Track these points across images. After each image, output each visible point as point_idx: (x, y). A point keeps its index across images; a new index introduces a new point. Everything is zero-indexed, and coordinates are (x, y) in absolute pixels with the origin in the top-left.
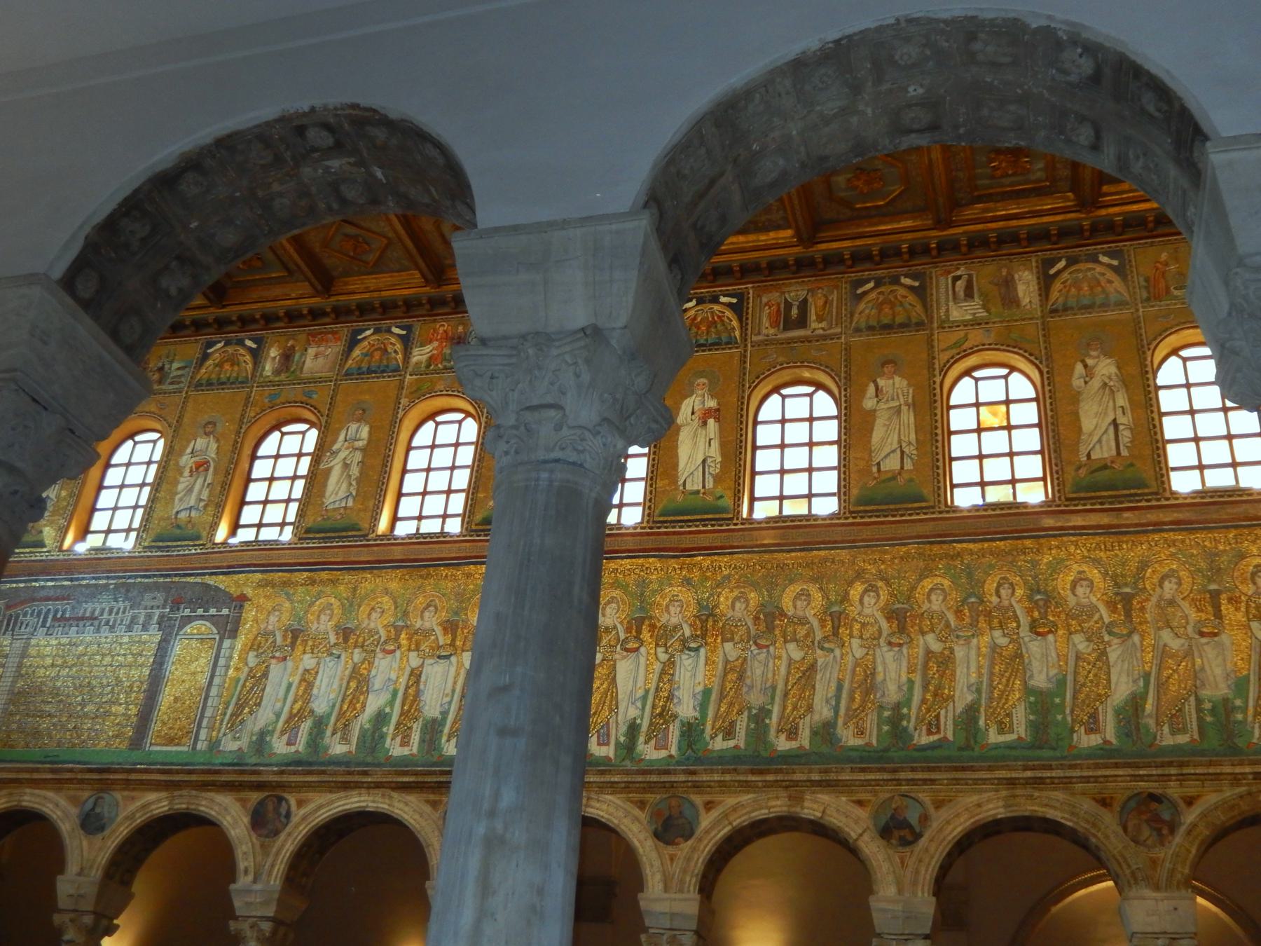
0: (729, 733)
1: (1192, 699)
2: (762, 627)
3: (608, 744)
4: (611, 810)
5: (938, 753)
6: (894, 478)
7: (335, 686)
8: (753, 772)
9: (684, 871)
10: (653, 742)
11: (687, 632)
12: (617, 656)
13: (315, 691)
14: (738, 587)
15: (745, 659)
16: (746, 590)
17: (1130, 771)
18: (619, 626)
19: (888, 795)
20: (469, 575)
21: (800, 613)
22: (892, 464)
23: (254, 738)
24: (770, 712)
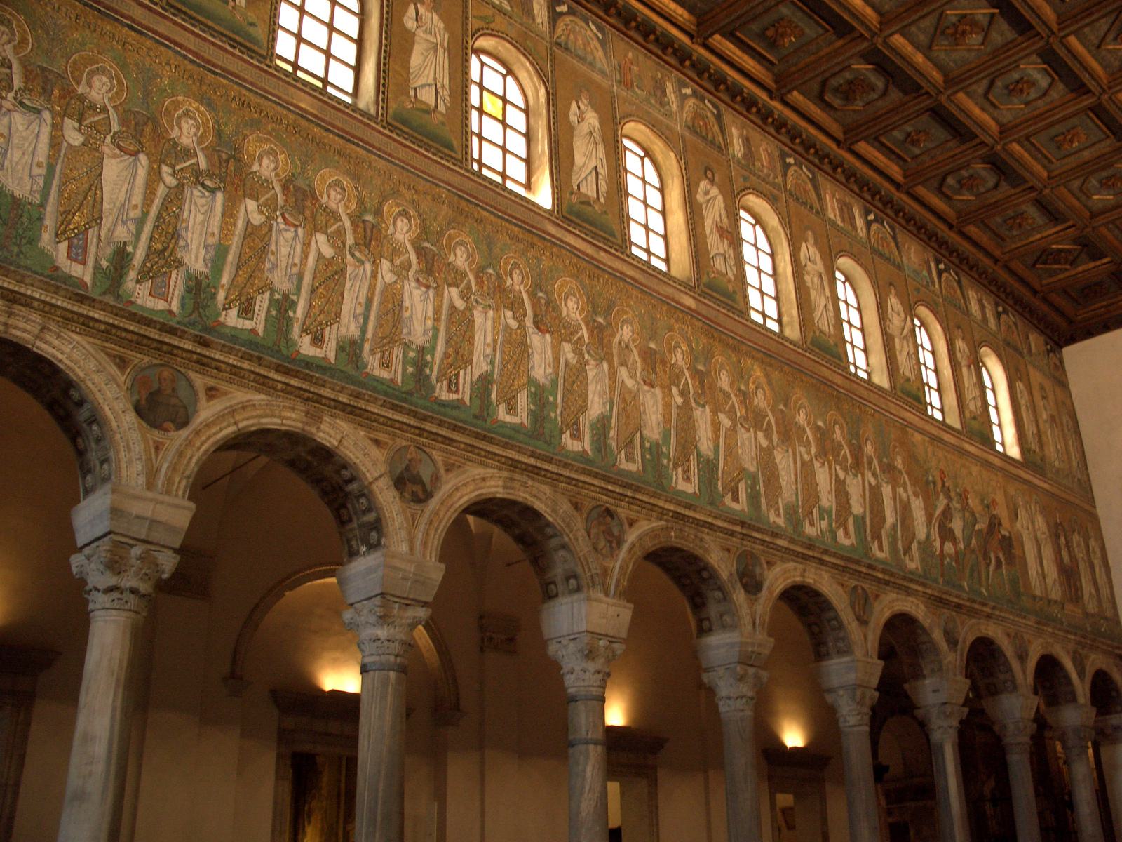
0: (247, 311)
1: (638, 434)
3: (84, 263)
4: (76, 355)
5: (455, 413)
6: (428, 112)
8: (278, 369)
9: (173, 468)
10: (148, 284)
11: (203, 165)
12: (106, 150)
14: (268, 140)
15: (270, 229)
17: (602, 484)
18: (111, 110)
19: (404, 443)
21: (333, 205)
22: (427, 96)
24: (293, 305)
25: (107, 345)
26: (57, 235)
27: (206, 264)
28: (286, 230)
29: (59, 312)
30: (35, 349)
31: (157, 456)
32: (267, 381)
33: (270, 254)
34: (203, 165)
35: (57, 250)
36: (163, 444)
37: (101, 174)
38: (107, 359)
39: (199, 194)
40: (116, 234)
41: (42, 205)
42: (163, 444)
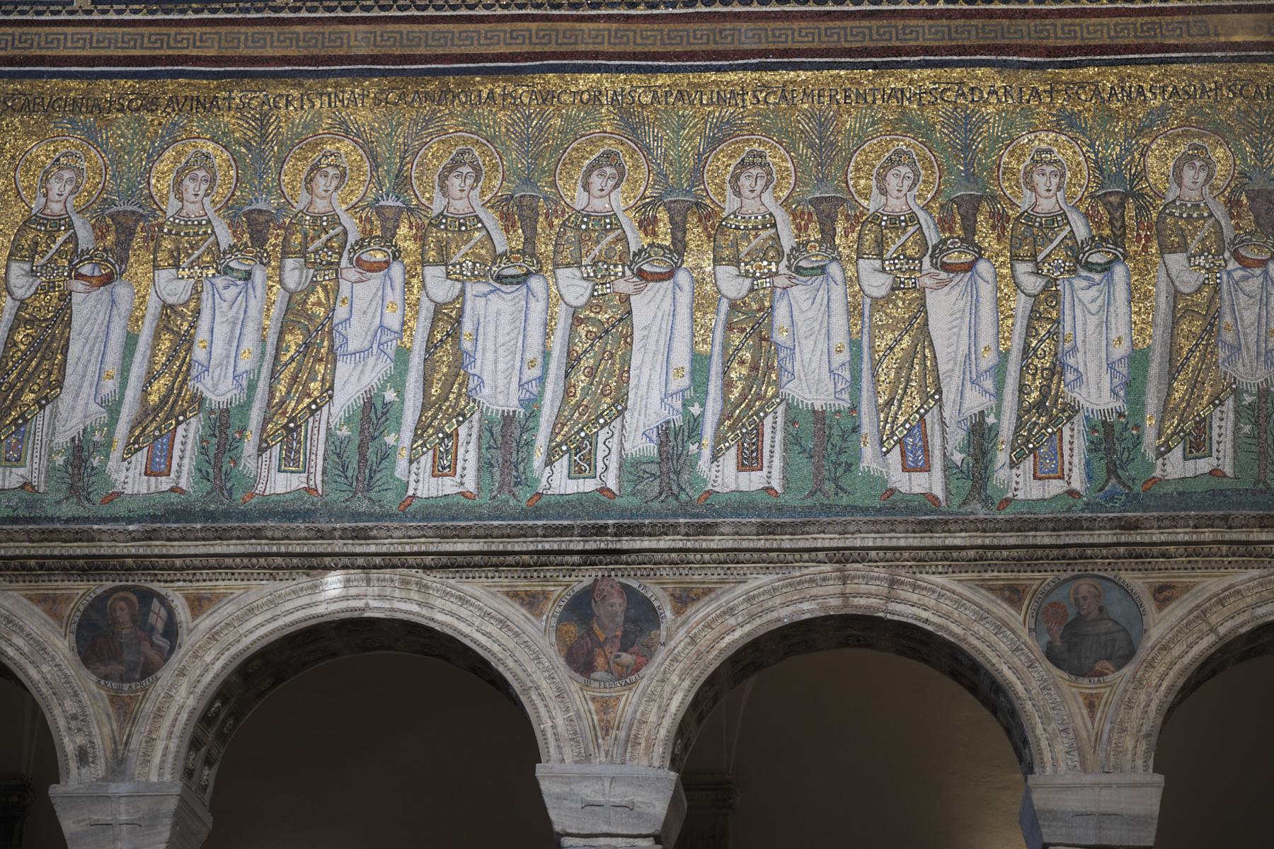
0: (1197, 444)
2: (1248, 222)
3: (927, 468)
7: (250, 342)
11: (1081, 232)
12: (927, 281)
13: (199, 353)
14: (1185, 135)
15: (1217, 289)
16: (1207, 142)
20: (547, 97)
23: (60, 460)
25: (986, 576)
26: (882, 443)
27: (1117, 394)
28: (1245, 278)
29: (906, 554)
30: (889, 616)
31: (1092, 718)
32: (1252, 547)
33: (1223, 332)
34: (1081, 232)
35: (887, 466)
36: (1099, 696)
37: (926, 324)
38: (993, 597)
39: (1085, 283)
40: (966, 405)
41: (854, 408)
42: (1099, 696)
